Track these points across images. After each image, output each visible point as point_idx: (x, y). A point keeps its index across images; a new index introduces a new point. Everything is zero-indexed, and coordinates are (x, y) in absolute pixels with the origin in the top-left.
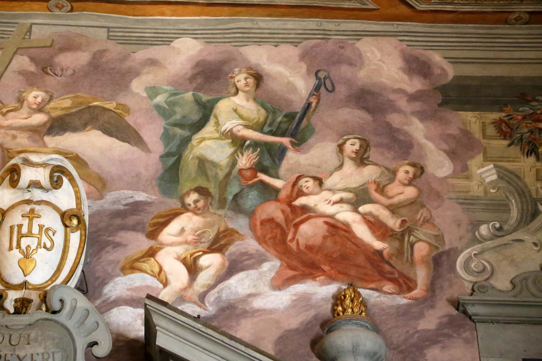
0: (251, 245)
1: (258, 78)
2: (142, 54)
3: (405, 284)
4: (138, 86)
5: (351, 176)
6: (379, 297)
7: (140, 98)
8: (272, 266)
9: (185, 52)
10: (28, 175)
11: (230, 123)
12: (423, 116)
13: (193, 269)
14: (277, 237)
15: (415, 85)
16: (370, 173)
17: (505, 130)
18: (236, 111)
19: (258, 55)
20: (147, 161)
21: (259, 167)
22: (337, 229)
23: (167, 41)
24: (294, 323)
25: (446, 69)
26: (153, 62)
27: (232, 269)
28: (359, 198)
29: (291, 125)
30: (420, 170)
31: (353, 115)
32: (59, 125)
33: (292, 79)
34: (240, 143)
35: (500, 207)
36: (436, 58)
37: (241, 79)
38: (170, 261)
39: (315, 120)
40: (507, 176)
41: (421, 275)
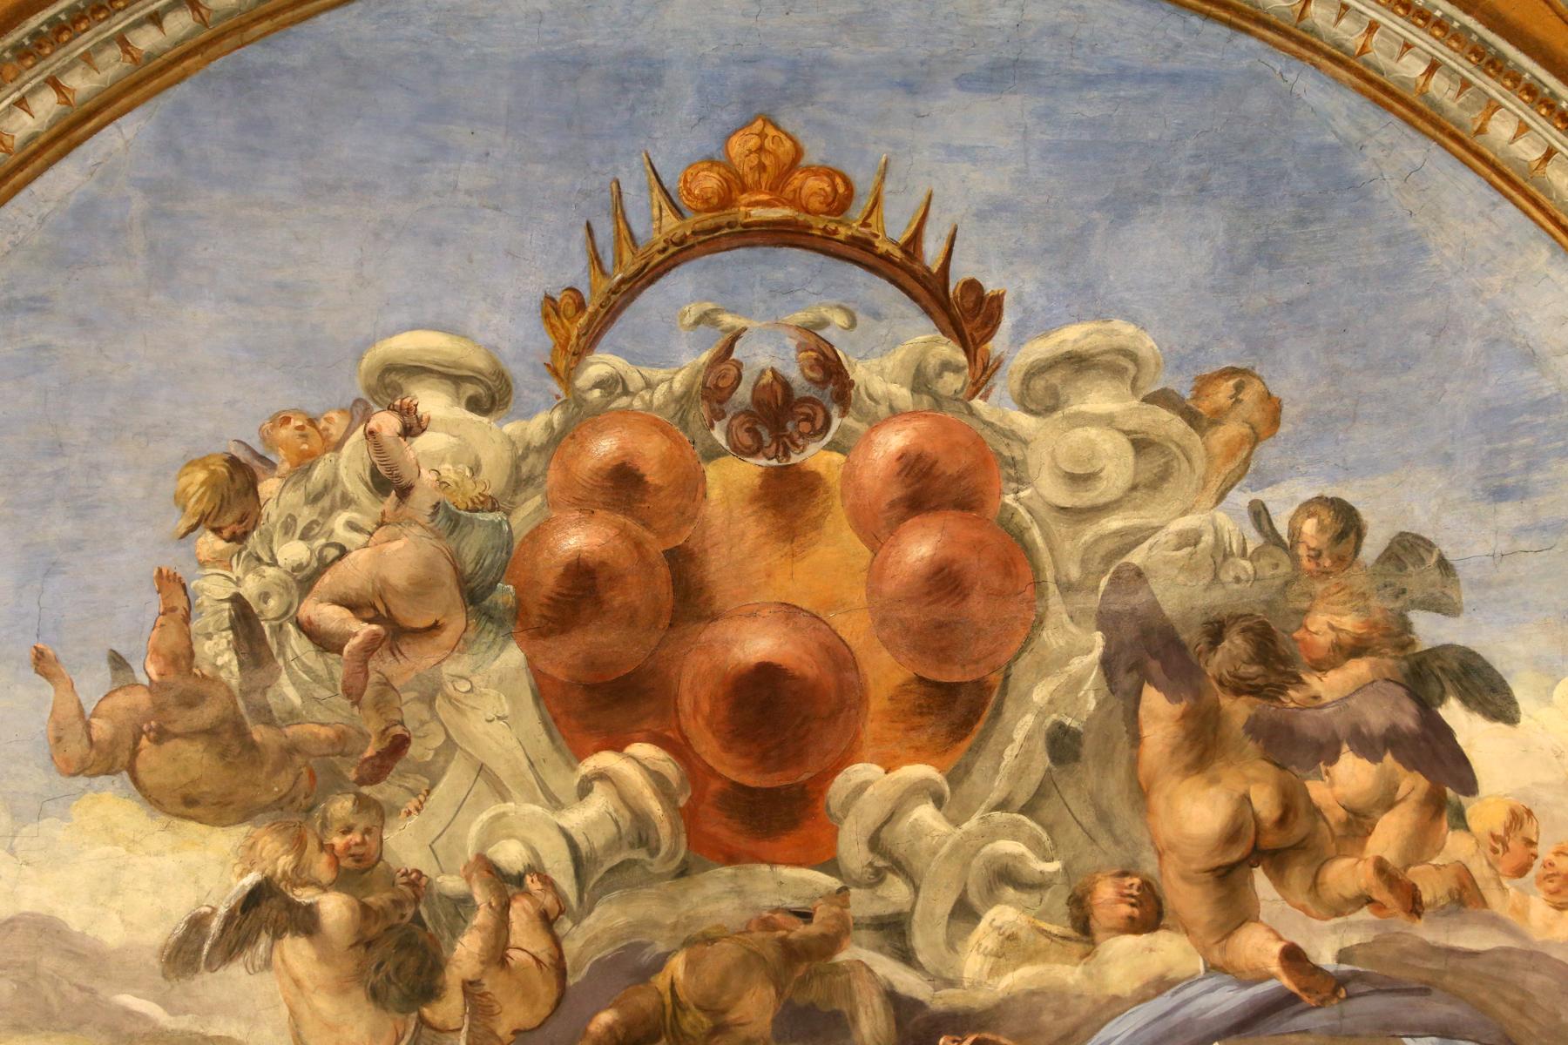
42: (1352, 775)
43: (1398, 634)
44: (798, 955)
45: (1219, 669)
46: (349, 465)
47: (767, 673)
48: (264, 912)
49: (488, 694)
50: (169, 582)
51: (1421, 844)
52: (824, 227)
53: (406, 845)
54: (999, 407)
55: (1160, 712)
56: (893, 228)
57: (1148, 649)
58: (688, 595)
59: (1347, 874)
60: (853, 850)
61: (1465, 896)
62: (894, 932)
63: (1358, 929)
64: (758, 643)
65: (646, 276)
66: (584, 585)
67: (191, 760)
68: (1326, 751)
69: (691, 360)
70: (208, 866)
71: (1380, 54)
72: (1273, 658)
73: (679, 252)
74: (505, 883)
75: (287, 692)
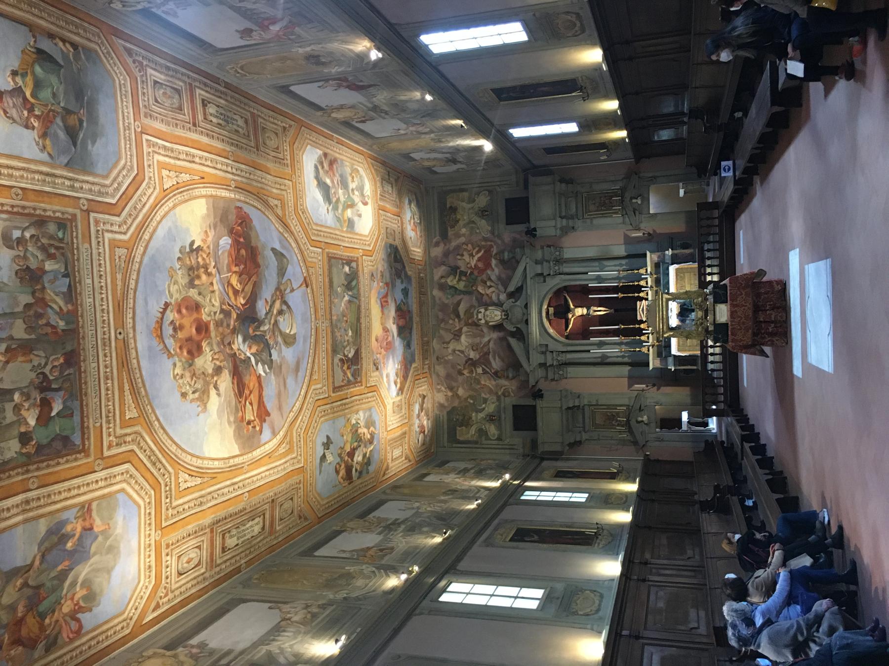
0: (484, 277)
1: (442, 277)
2: (438, 301)
3: (491, 246)
4: (446, 302)
5: (466, 257)
6: (495, 251)
7: (449, 300)
8: (489, 272)
9: (436, 292)
10: (480, 317)
11: (455, 282)
12: (450, 242)
13: (491, 287)
14: (482, 271)
15: (442, 245)
16: (465, 253)
17: (453, 227)
18: (451, 281)
19: (436, 278)
20: (466, 298)
21: (465, 275)
22: (479, 260)
23: (434, 297)
24: (501, 267)
25: (438, 238)
26: (440, 299)
27: (490, 279)
28: (472, 255)
29: (454, 270)
30: (464, 243)
31: (451, 257)
32: (458, 316)
33: (442, 270)
34: (460, 280)
35: (472, 228)
36: (434, 240)
37: (443, 280)
38: (489, 291)
39: (452, 264)
40: (464, 226)
41: (489, 243)
42: (200, 260)
43: (188, 253)
44: (218, 324)
45: (193, 273)
46: (181, 381)
47: (196, 329)
48: (216, 388)
49: (199, 362)
50: (192, 401)
51: (205, 252)
52: (160, 322)
53: (210, 371)
54: (173, 301)
55: (197, 282)
56: (159, 315)
57: (191, 284)
58: (189, 339)
59: (208, 261)
60: (209, 319)
61: (208, 247)
62: (215, 313)
63: (212, 260)
64: (194, 330)
65: (165, 346)
66: (190, 352)
67: (205, 396)
68: (198, 262)
69: (172, 340)
70: (213, 392)
71: (141, 253)
72: (191, 269)
73: (164, 342)
74: (213, 359)
75: (199, 386)
